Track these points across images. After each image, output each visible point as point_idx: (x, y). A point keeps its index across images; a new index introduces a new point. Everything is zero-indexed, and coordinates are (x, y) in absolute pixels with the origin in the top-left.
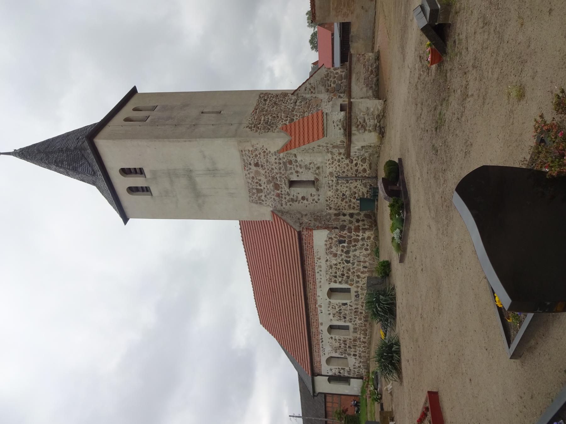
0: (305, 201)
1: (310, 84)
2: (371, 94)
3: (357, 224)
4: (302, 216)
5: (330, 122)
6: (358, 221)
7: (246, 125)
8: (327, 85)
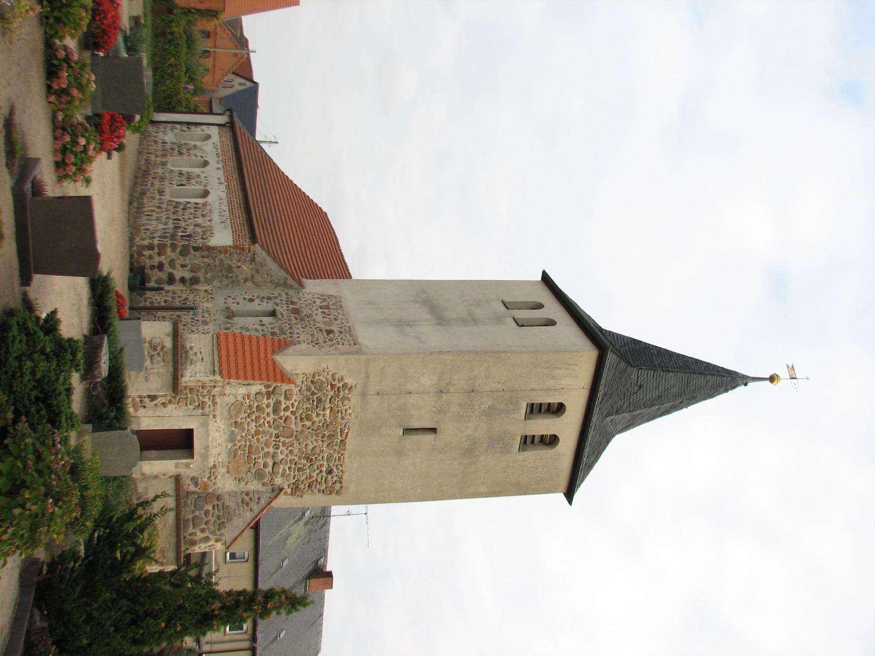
0: (247, 297)
1: (251, 510)
2: (139, 484)
3: (162, 259)
4: (252, 277)
5: (208, 360)
6: (160, 266)
7: (355, 392)
8: (220, 507)
